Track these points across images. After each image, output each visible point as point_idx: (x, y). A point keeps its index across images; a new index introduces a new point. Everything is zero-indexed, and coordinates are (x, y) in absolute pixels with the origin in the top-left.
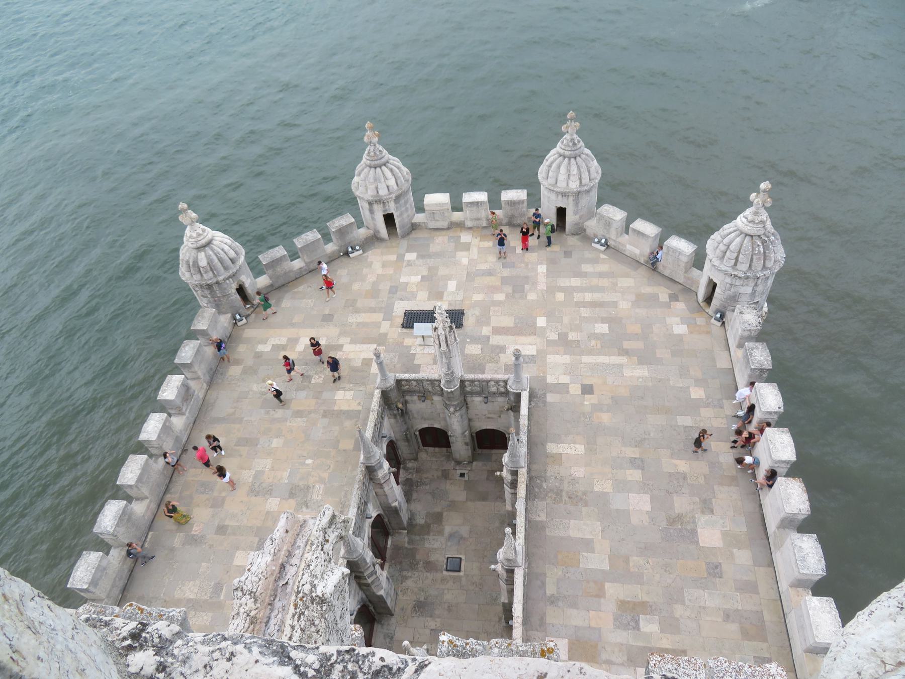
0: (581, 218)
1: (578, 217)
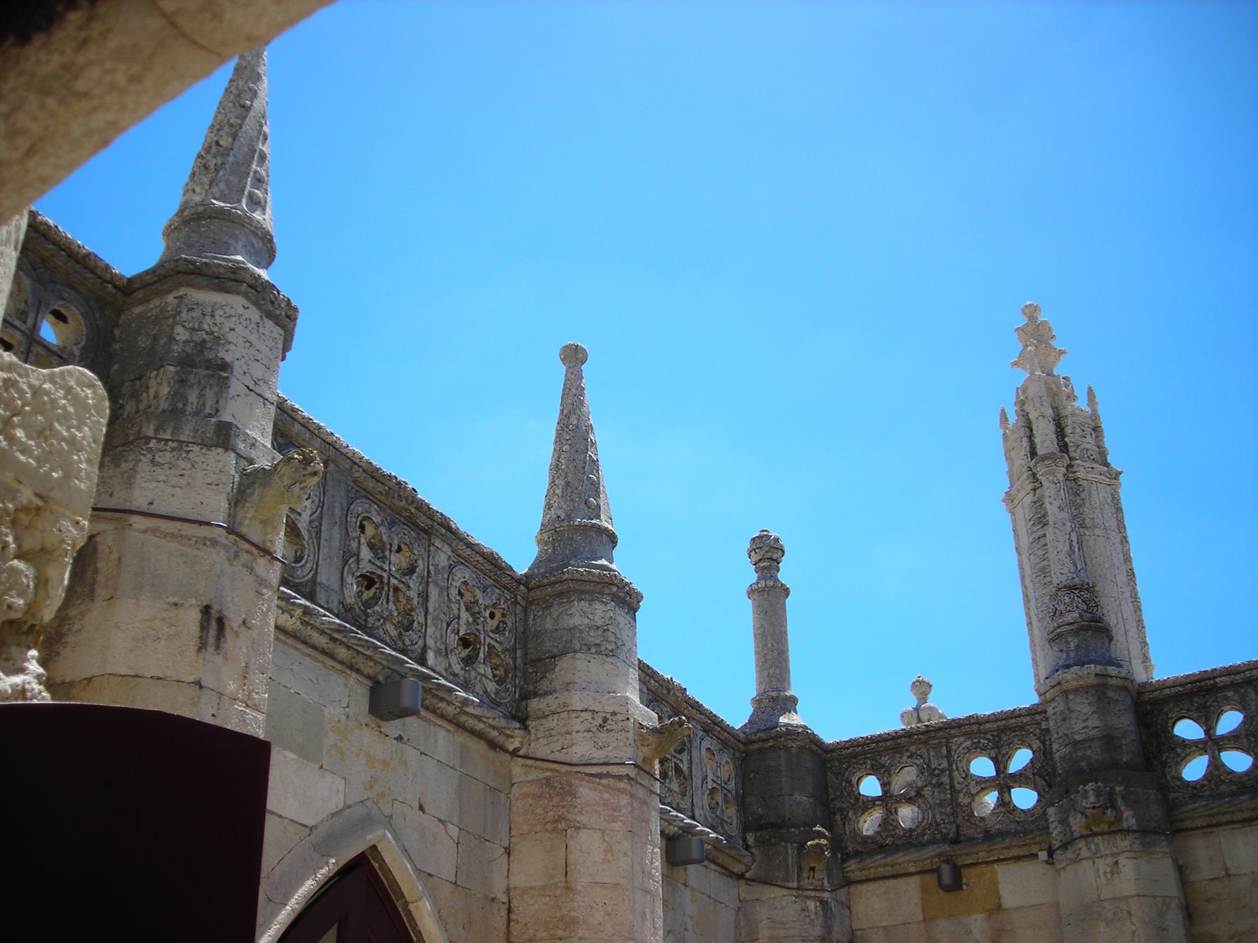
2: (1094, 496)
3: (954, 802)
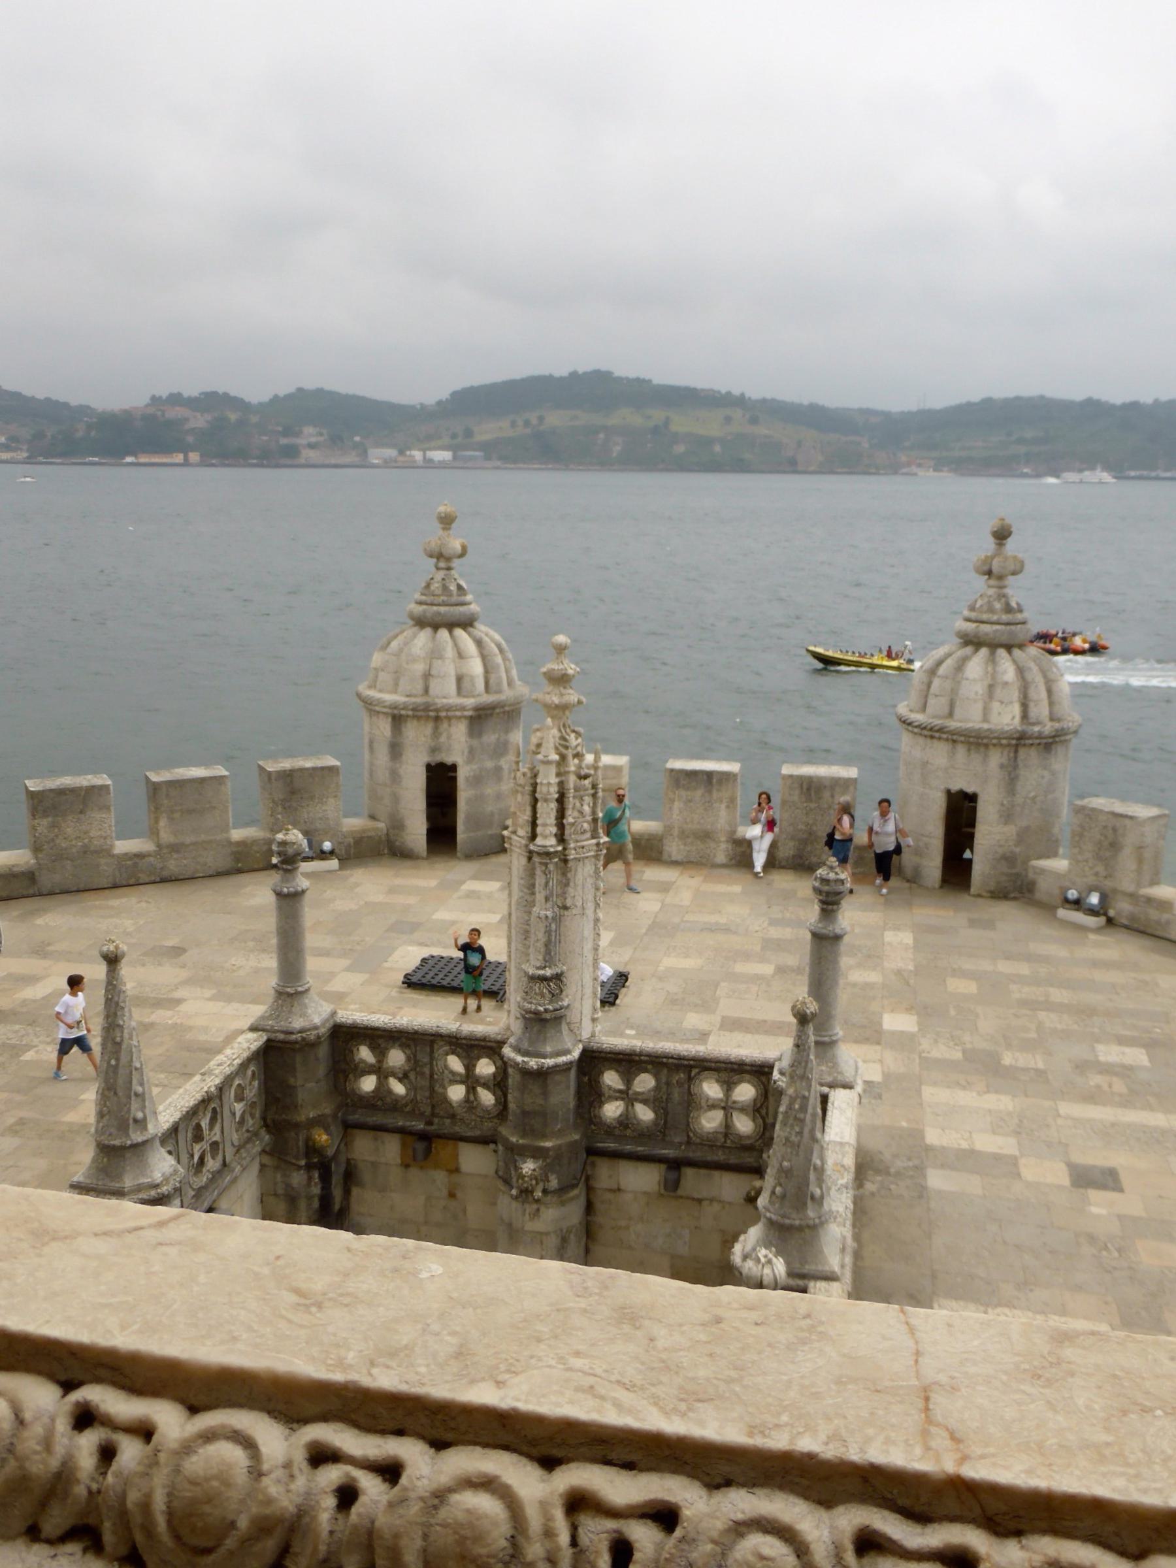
0: (1021, 837)
1: (1011, 830)
2: (579, 878)
3: (432, 1089)
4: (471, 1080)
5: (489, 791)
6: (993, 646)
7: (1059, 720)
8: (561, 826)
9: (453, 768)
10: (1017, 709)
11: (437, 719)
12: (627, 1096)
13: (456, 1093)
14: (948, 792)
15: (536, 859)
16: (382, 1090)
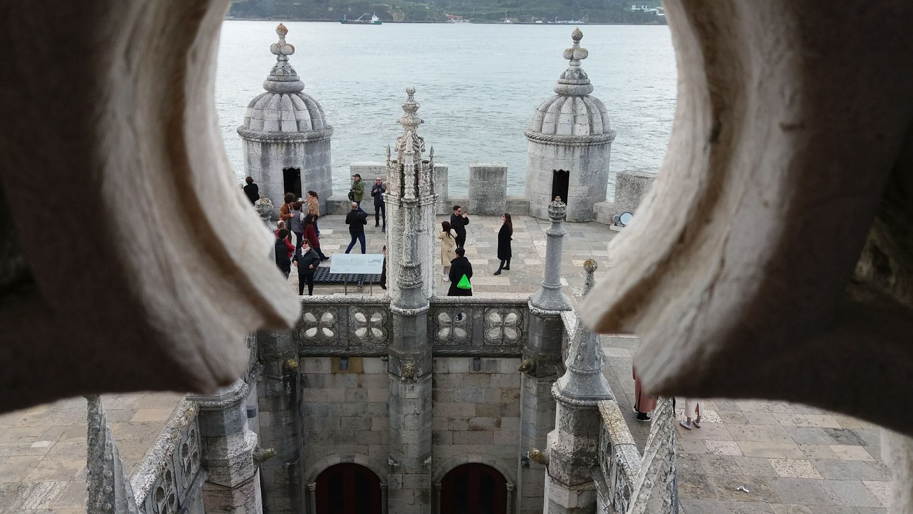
0: (590, 192)
1: (585, 188)
4: (369, 325)
5: (318, 182)
6: (574, 96)
7: (607, 133)
8: (417, 188)
9: (299, 170)
10: (588, 128)
11: (288, 144)
12: (451, 325)
13: (360, 332)
14: (555, 171)
15: (405, 205)
16: (320, 334)
